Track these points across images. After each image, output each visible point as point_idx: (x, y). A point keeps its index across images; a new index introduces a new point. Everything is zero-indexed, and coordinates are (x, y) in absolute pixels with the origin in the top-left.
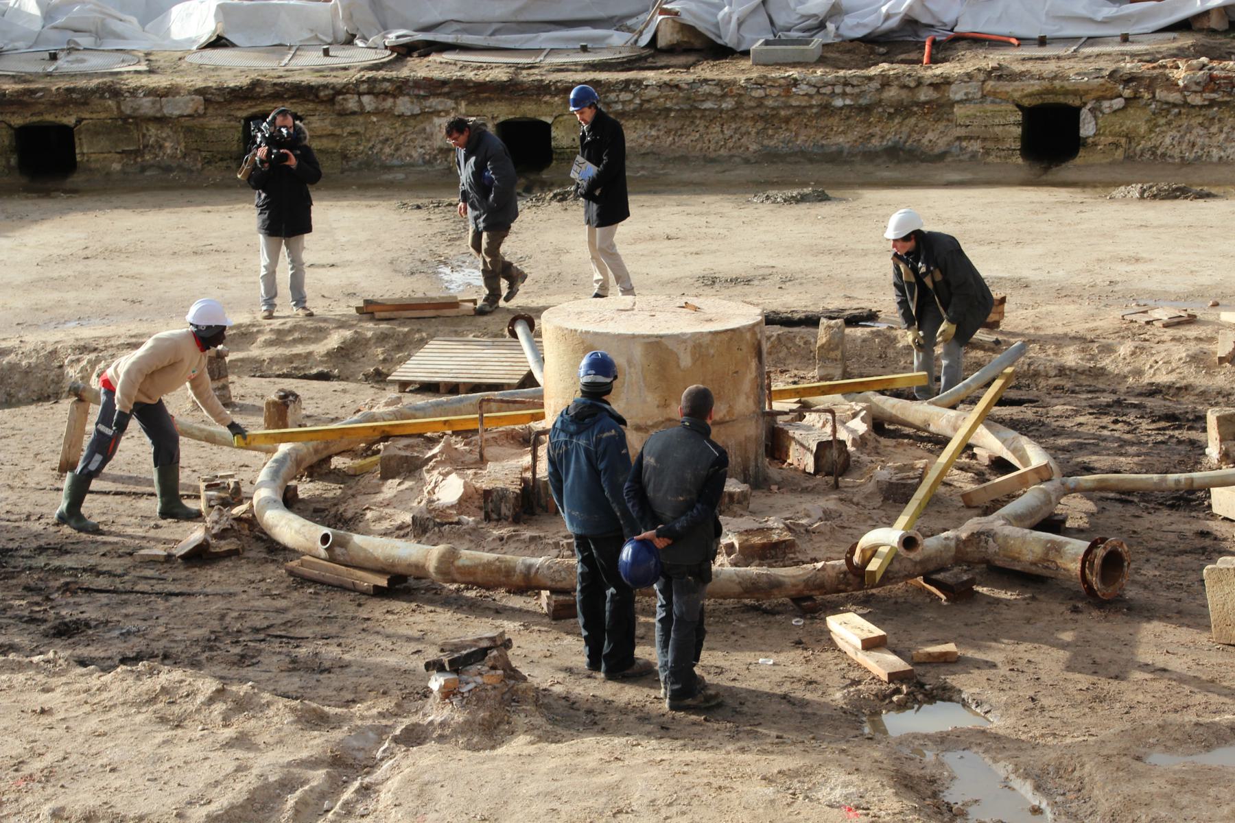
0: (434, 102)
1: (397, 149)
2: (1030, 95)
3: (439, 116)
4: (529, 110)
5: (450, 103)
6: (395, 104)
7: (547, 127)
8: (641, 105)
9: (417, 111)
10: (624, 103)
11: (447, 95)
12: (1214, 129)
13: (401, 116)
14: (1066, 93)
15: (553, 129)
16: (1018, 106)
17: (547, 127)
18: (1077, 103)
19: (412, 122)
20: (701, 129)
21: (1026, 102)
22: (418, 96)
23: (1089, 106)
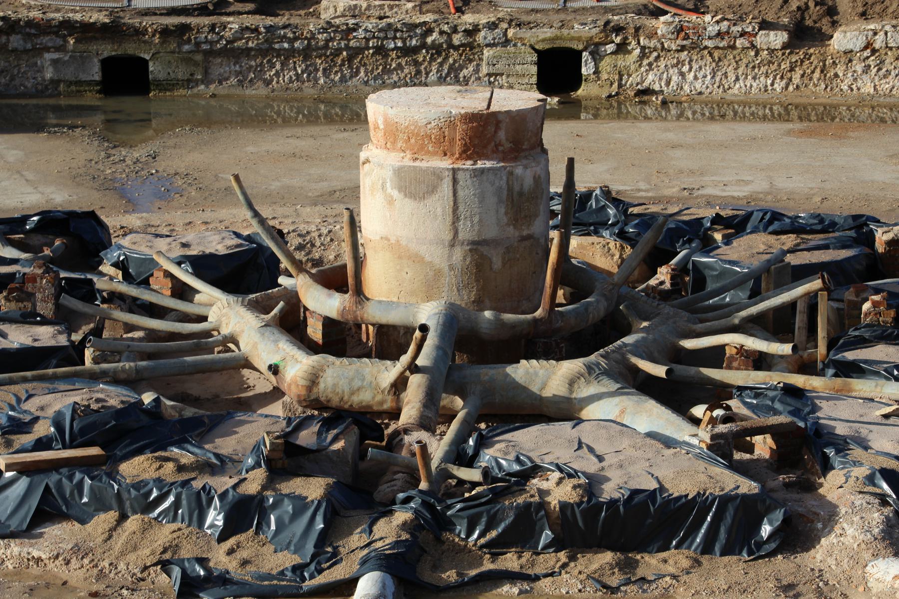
0: (46, 40)
1: (12, 79)
2: (543, 40)
3: (49, 52)
4: (130, 48)
5: (59, 42)
6: (8, 40)
7: (146, 62)
8: (226, 45)
9: (29, 46)
10: (211, 43)
11: (56, 34)
12: (685, 69)
13: (14, 50)
14: (572, 39)
15: (151, 64)
16: (533, 48)
17: (146, 62)
18: (581, 47)
19: (25, 57)
20: (278, 66)
21: (539, 47)
22: (29, 34)
23: (590, 50)
